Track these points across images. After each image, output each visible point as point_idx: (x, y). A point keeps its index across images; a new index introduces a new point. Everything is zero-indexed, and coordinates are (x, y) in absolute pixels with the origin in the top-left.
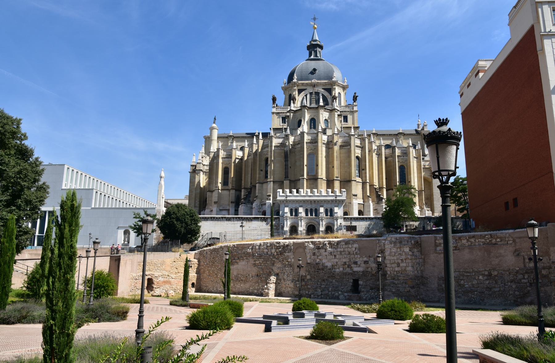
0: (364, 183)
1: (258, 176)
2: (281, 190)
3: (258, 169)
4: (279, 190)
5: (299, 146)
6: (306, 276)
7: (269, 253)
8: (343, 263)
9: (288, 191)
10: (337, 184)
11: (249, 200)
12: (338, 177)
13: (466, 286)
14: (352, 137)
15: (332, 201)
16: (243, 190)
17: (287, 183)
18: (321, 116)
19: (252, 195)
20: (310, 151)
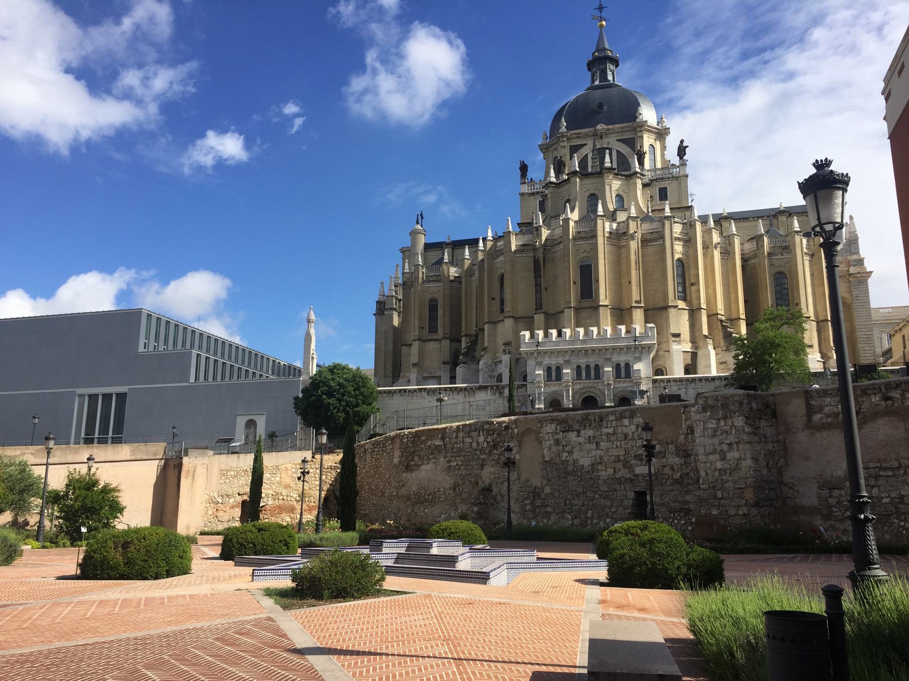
0: (694, 313)
2: (527, 334)
5: (561, 246)
6: (543, 489)
7: (474, 445)
8: (613, 458)
9: (540, 333)
10: (638, 315)
11: (474, 357)
12: (639, 302)
13: (885, 500)
14: (667, 223)
15: (629, 348)
16: (463, 339)
17: (539, 318)
18: (607, 188)
19: (479, 347)
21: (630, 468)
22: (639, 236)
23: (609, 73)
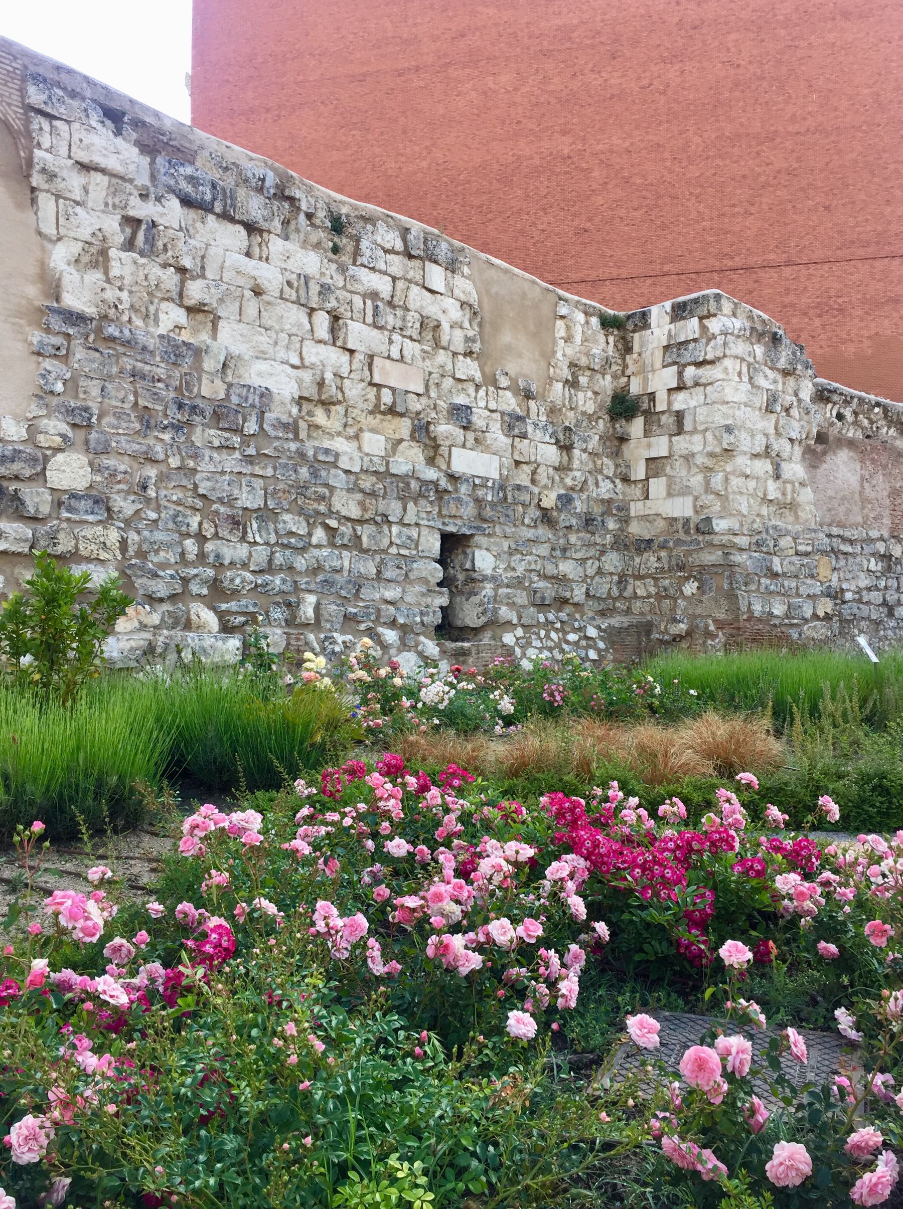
21: (434, 450)
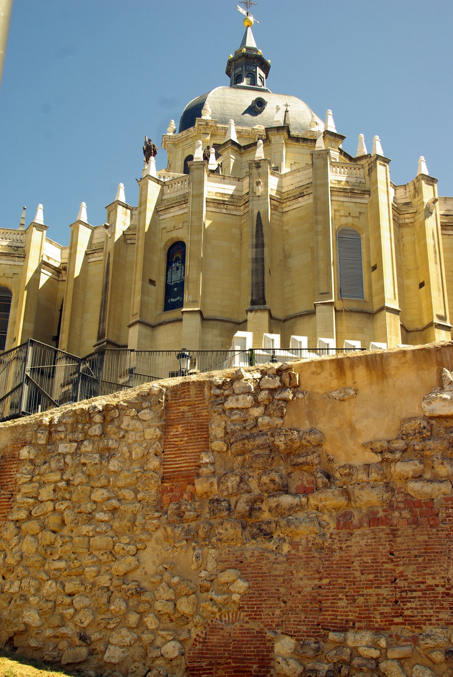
1: (138, 298)
3: (139, 275)
4: (239, 334)
12: (443, 318)
20: (344, 221)
22: (439, 210)
23: (258, 79)
